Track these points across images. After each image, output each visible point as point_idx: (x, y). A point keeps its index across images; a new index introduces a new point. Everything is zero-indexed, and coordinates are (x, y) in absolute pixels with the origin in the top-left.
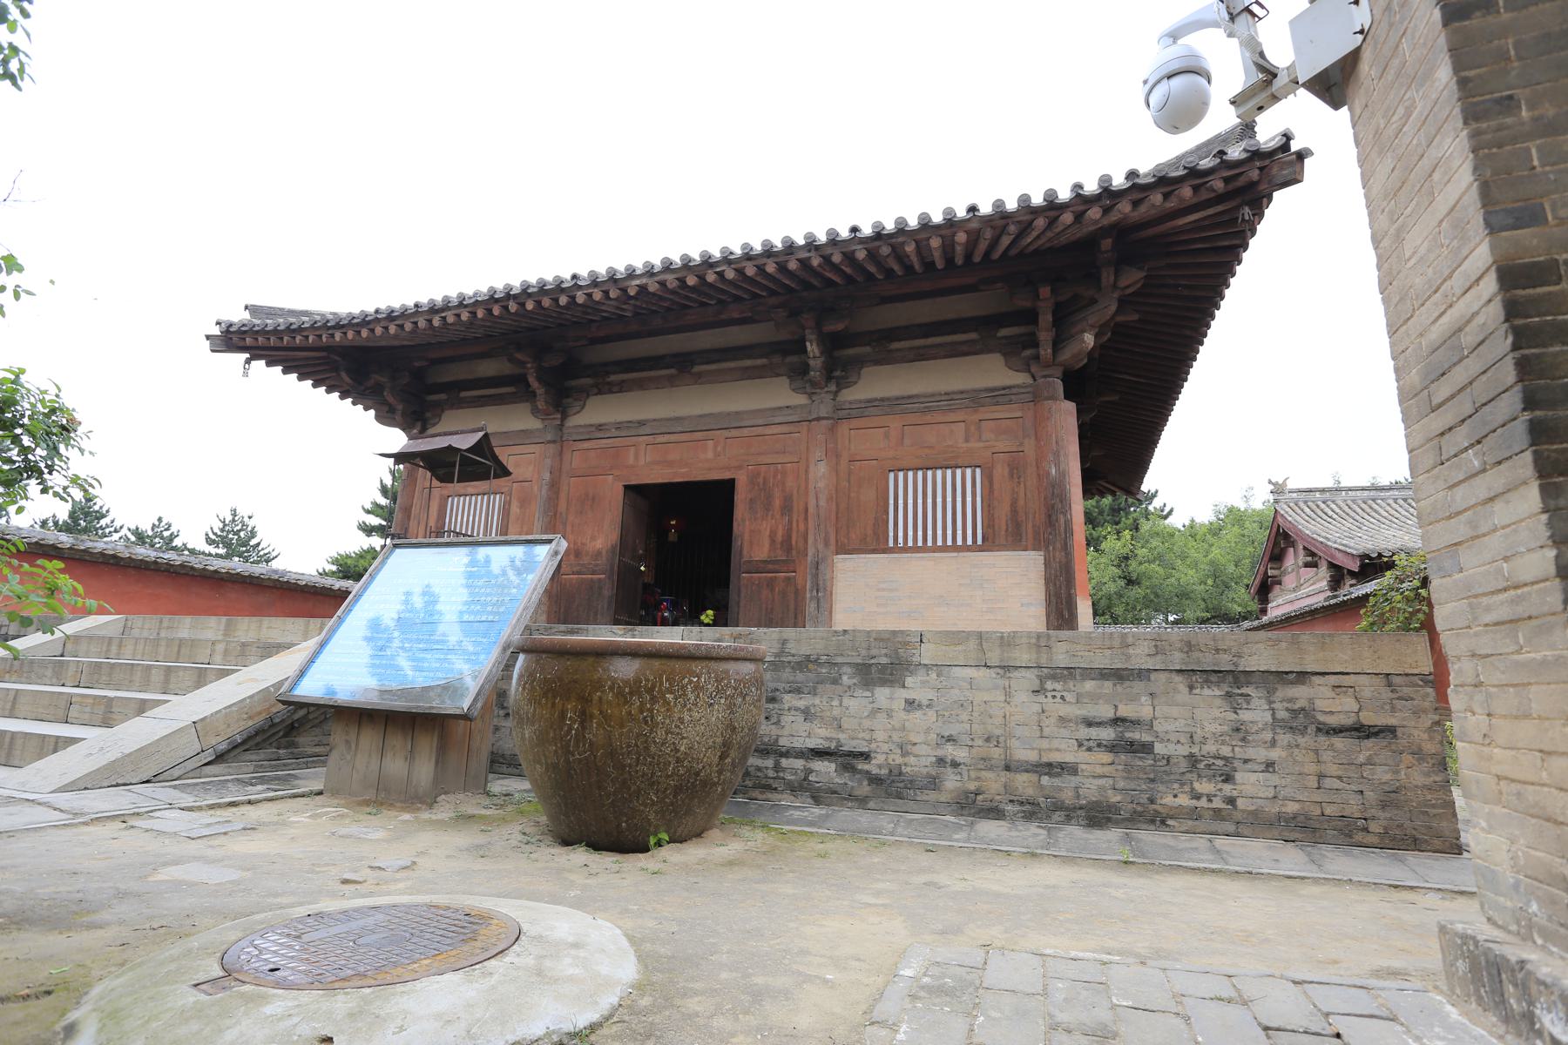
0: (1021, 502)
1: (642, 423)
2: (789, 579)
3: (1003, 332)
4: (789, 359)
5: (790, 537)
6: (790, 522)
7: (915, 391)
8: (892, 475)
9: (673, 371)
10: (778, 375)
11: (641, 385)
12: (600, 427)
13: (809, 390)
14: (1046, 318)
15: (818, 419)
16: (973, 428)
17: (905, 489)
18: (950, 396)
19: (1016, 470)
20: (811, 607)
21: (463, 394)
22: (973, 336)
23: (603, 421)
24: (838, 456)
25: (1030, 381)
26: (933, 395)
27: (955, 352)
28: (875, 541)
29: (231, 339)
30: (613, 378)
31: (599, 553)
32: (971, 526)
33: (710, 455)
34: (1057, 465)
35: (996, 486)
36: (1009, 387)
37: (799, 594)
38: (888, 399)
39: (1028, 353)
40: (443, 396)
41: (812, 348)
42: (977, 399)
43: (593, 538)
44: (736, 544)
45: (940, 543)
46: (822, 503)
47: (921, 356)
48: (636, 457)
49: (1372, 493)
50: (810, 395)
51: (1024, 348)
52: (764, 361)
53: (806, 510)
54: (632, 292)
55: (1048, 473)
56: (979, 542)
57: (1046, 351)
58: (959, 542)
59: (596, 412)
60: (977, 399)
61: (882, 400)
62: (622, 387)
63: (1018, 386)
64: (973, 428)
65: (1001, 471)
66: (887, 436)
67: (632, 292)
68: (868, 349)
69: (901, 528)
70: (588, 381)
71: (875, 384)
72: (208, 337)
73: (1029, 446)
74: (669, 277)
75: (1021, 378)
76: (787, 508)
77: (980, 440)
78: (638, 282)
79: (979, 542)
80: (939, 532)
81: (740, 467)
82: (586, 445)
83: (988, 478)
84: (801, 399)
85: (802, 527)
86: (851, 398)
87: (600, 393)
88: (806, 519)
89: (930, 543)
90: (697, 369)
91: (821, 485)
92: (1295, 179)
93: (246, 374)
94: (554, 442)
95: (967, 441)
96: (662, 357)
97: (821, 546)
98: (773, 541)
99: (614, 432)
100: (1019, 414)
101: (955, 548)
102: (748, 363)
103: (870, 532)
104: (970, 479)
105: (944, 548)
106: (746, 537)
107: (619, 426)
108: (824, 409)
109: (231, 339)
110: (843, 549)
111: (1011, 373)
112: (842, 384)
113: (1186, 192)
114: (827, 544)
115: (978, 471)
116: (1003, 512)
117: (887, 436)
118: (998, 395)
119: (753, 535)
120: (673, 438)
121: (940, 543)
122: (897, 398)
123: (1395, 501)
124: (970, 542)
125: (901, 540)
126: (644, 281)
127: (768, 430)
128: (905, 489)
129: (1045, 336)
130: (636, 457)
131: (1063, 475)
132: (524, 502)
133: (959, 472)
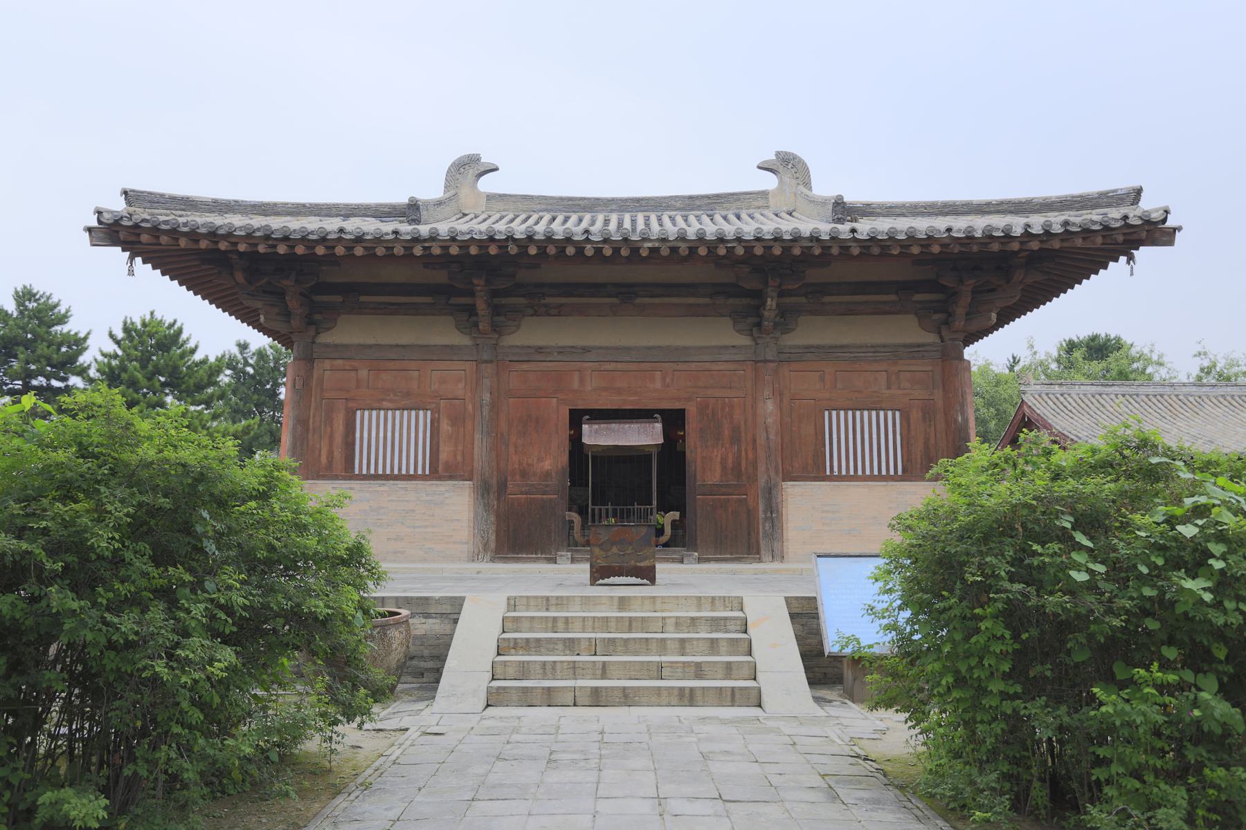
0: (932, 441)
1: (586, 350)
2: (740, 500)
3: (918, 297)
4: (731, 301)
5: (740, 464)
6: (739, 451)
7: (845, 342)
8: (827, 413)
9: (614, 300)
10: (722, 316)
11: (581, 311)
12: (539, 350)
13: (756, 334)
14: (965, 300)
15: (765, 361)
16: (893, 378)
17: (838, 424)
18: (875, 348)
19: (928, 414)
20: (763, 527)
21: (363, 299)
22: (893, 297)
23: (541, 343)
24: (781, 395)
25: (938, 340)
26: (861, 347)
27: (879, 311)
28: (816, 470)
29: (111, 232)
30: (548, 300)
31: (547, 475)
32: (894, 460)
33: (658, 385)
34: (963, 413)
35: (912, 427)
36: (923, 345)
37: (751, 514)
38: (823, 347)
39: (936, 317)
40: (339, 298)
41: (771, 303)
42: (896, 352)
43: (540, 460)
44: (689, 470)
45: (868, 472)
46: (772, 437)
47: (850, 311)
48: (582, 381)
49: (1100, 388)
50: (755, 339)
51: (935, 312)
52: (706, 300)
53: (754, 441)
54: (644, 253)
55: (956, 421)
56: (900, 473)
57: (959, 323)
58: (884, 473)
59: (531, 334)
60: (896, 352)
61: (818, 347)
62: (560, 311)
63: (929, 345)
64: (893, 378)
65: (916, 415)
66: (822, 379)
67: (644, 253)
68: (803, 300)
69: (836, 460)
70: (522, 300)
71: (811, 333)
72: (89, 230)
73: (938, 395)
74: (683, 246)
75: (931, 338)
76: (736, 438)
77: (899, 388)
78: (650, 245)
79: (900, 473)
80: (867, 463)
81: (689, 399)
82: (525, 366)
83: (906, 419)
84: (744, 340)
85: (750, 456)
86: (790, 343)
87: (535, 314)
88: (755, 448)
89: (860, 473)
90: (639, 301)
91: (770, 420)
92: (1170, 242)
93: (131, 272)
94: (491, 362)
95: (889, 388)
96: (604, 285)
97: (772, 474)
98: (724, 468)
99: (556, 357)
100: (930, 368)
101: (880, 478)
102: (691, 300)
103: (810, 462)
104: (892, 419)
105: (872, 478)
106: (699, 462)
107: (562, 350)
108: (770, 354)
109: (111, 232)
110: (789, 477)
111: (923, 333)
112: (786, 331)
113: (1099, 240)
114: (777, 473)
115: (897, 414)
116: (918, 449)
117: (822, 379)
118: (915, 350)
119: (706, 463)
120: (619, 366)
121: (868, 472)
122: (831, 347)
123: (1116, 395)
124: (892, 472)
125: (836, 469)
126: (657, 245)
127: (715, 367)
128: (838, 424)
129: (960, 311)
130: (582, 381)
131: (966, 421)
132: (458, 420)
133: (882, 413)
